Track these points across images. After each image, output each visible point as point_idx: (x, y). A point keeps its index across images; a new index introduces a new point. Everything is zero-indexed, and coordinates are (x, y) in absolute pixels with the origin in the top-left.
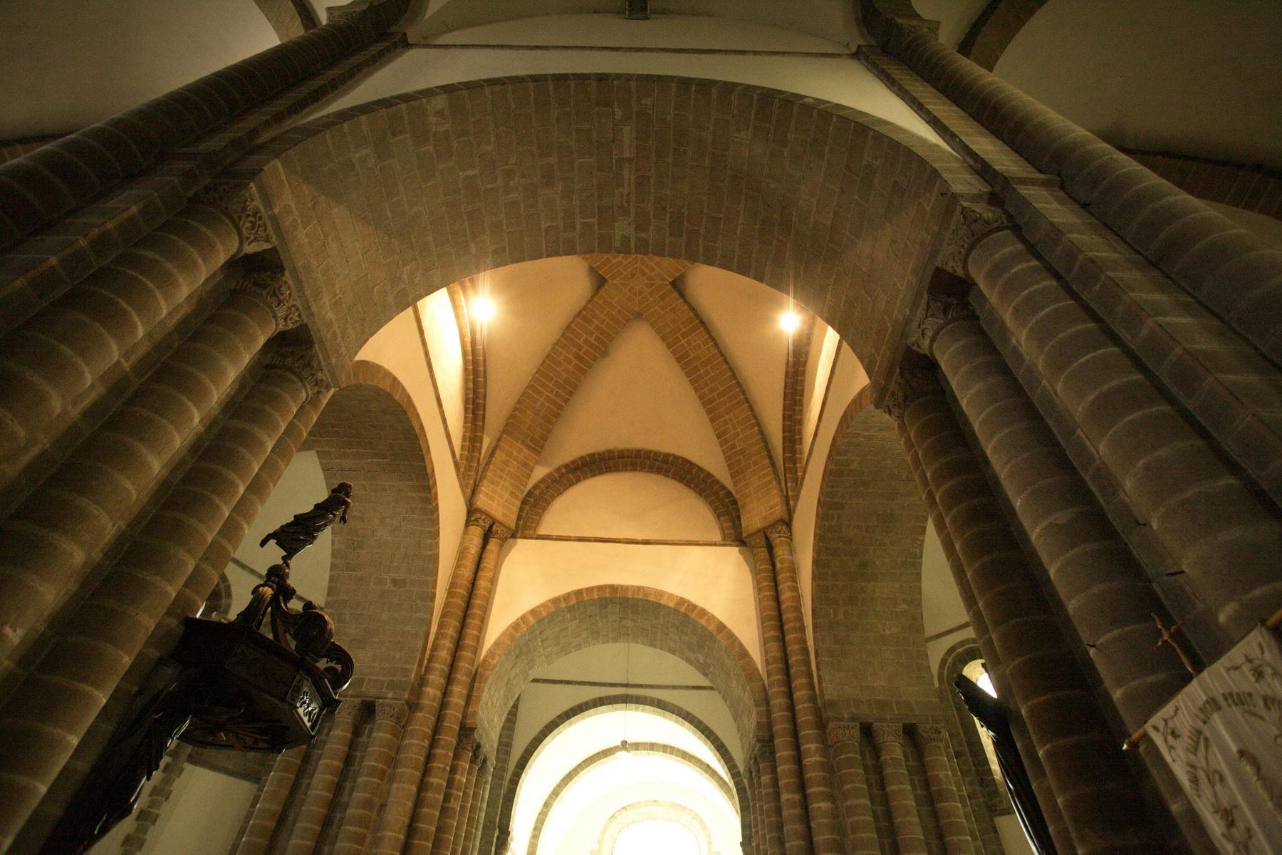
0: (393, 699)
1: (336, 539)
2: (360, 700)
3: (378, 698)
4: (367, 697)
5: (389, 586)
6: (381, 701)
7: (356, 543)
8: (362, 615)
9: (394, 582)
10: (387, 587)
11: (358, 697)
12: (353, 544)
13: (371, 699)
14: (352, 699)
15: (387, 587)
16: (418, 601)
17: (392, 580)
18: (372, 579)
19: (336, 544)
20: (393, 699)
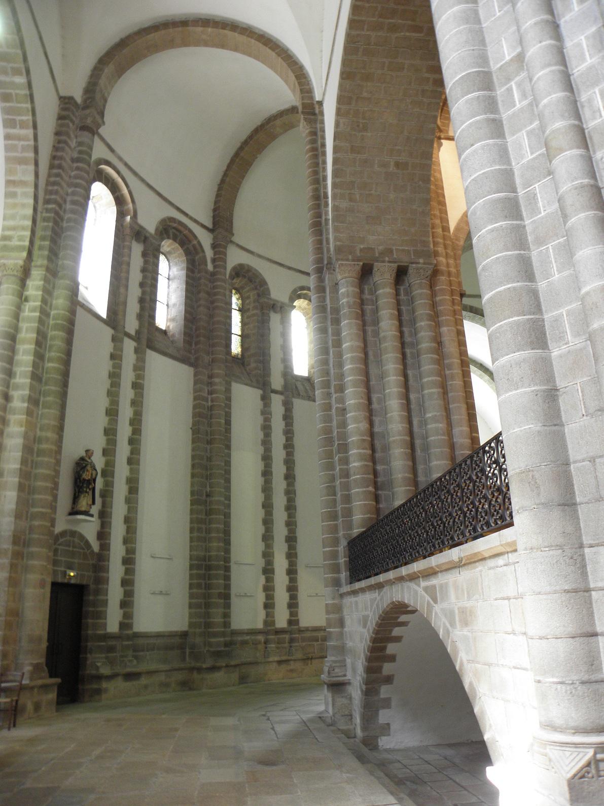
0: (424, 264)
1: (341, 121)
2: (396, 265)
3: (412, 263)
4: (402, 262)
5: (392, 168)
6: (414, 265)
7: (361, 125)
8: (371, 194)
9: (397, 165)
10: (391, 169)
11: (395, 262)
12: (358, 126)
13: (406, 264)
14: (390, 264)
15: (391, 169)
16: (421, 182)
17: (395, 162)
18: (376, 162)
19: (341, 125)
20: (424, 264)
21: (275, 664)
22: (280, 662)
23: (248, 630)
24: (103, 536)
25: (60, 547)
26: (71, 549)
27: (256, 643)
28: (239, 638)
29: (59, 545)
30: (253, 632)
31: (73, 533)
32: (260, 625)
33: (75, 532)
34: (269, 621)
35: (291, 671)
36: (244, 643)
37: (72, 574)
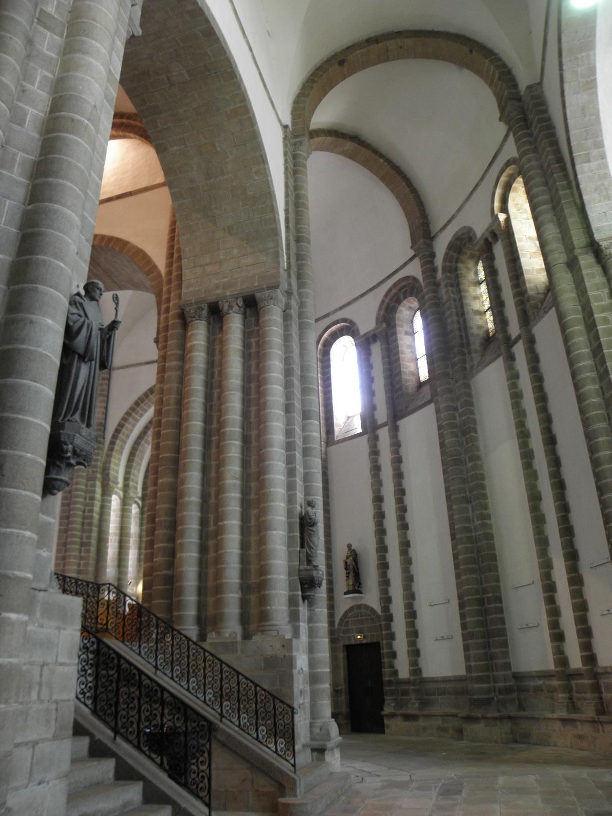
21: (558, 724)
22: (564, 721)
23: (536, 672)
24: (386, 600)
25: (350, 620)
26: (360, 618)
27: (552, 690)
28: (532, 684)
29: (349, 618)
30: (545, 675)
31: (359, 607)
32: (551, 666)
33: (361, 605)
34: (562, 660)
35: (580, 737)
36: (538, 689)
37: (359, 637)
